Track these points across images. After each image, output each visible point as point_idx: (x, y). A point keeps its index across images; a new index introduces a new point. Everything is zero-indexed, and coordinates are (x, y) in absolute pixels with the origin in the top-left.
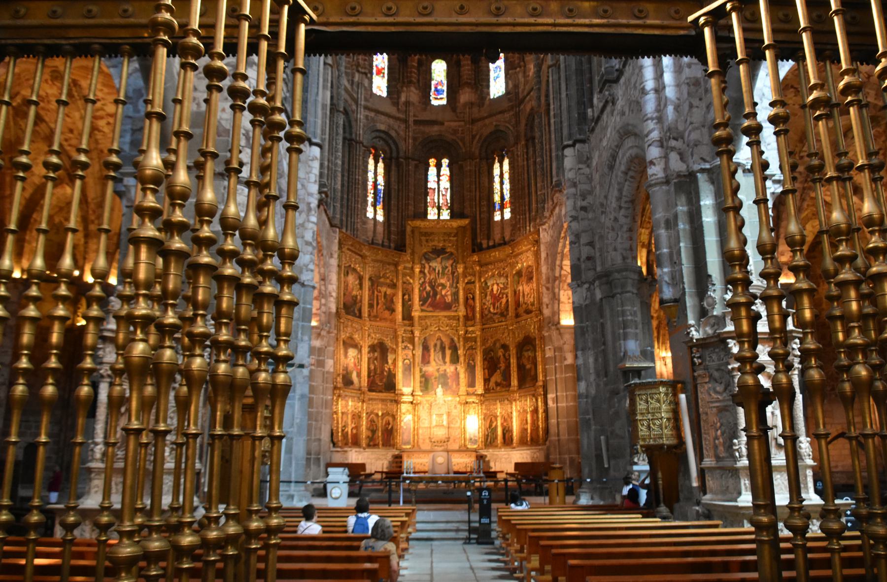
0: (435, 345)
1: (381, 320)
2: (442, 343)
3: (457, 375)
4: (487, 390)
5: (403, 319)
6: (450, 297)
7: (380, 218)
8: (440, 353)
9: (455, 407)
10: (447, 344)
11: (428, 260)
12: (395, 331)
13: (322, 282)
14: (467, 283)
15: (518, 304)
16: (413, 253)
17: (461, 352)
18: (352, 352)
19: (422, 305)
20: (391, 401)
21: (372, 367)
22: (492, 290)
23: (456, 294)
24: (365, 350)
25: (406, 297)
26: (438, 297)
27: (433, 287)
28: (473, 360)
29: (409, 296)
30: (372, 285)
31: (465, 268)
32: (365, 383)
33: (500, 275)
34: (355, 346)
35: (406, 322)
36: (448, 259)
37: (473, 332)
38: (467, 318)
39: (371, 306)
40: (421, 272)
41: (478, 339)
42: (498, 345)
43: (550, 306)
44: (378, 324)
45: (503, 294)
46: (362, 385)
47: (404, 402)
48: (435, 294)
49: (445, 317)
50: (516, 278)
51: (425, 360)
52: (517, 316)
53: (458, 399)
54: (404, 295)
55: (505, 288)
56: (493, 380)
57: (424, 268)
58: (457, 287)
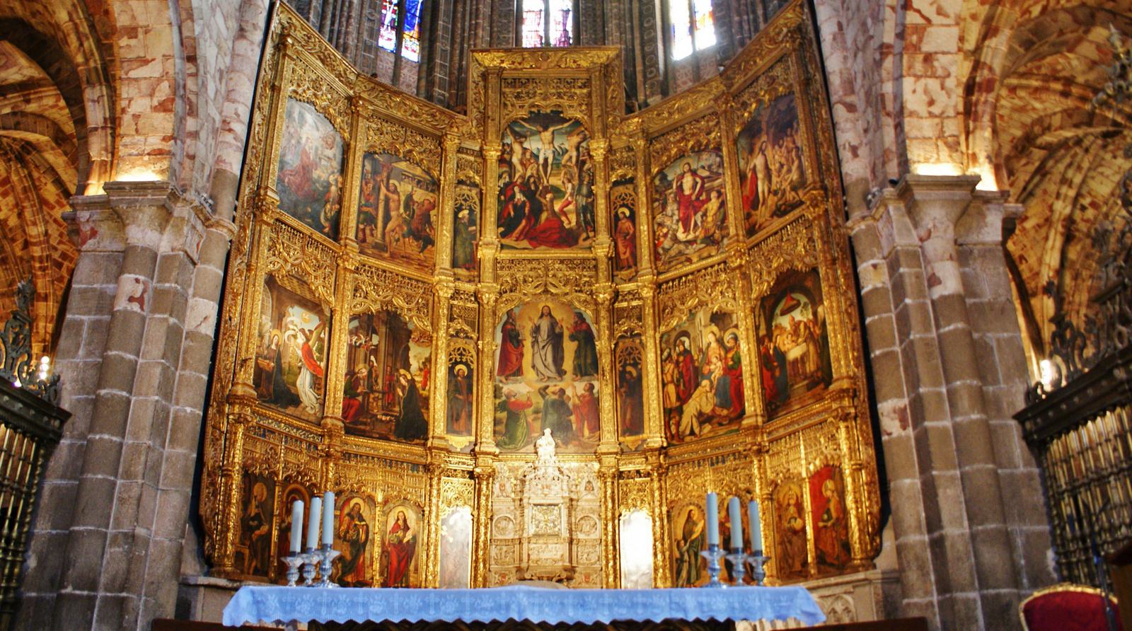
0: (537, 330)
1: (393, 257)
2: (553, 323)
3: (592, 403)
4: (675, 438)
5: (454, 264)
6: (573, 218)
7: (412, 51)
8: (549, 349)
9: (589, 487)
10: (566, 322)
11: (520, 137)
12: (430, 290)
13: (190, 68)
14: (616, 184)
15: (752, 202)
16: (484, 120)
17: (603, 345)
18: (299, 318)
19: (503, 235)
20: (415, 466)
21: (362, 370)
22: (680, 188)
23: (588, 211)
24: (343, 324)
25: (464, 213)
26: (544, 216)
27: (530, 194)
28: (635, 365)
29: (471, 211)
30: (375, 172)
31: (610, 150)
32: (336, 407)
33: (699, 150)
34: (314, 306)
35: (462, 272)
36: (569, 134)
37: (635, 295)
38: (615, 263)
39: (367, 219)
40: (501, 161)
41: (648, 311)
42: (702, 317)
43: (863, 151)
44: (384, 265)
45: (709, 192)
46: (328, 412)
47: (452, 473)
48: (537, 209)
49: (562, 262)
50: (743, 142)
51: (510, 365)
52: (751, 231)
53: (596, 466)
54: (458, 209)
55: (715, 175)
56: (691, 409)
57: (512, 152)
58: (590, 194)
